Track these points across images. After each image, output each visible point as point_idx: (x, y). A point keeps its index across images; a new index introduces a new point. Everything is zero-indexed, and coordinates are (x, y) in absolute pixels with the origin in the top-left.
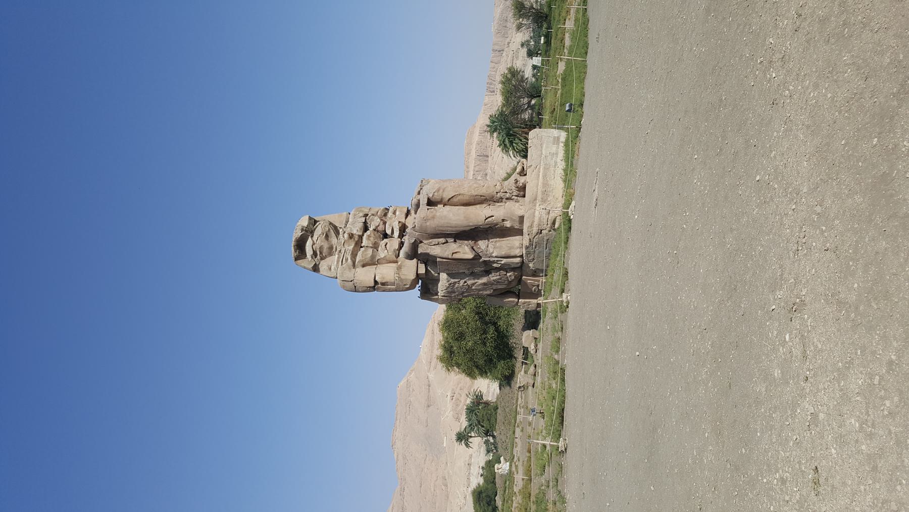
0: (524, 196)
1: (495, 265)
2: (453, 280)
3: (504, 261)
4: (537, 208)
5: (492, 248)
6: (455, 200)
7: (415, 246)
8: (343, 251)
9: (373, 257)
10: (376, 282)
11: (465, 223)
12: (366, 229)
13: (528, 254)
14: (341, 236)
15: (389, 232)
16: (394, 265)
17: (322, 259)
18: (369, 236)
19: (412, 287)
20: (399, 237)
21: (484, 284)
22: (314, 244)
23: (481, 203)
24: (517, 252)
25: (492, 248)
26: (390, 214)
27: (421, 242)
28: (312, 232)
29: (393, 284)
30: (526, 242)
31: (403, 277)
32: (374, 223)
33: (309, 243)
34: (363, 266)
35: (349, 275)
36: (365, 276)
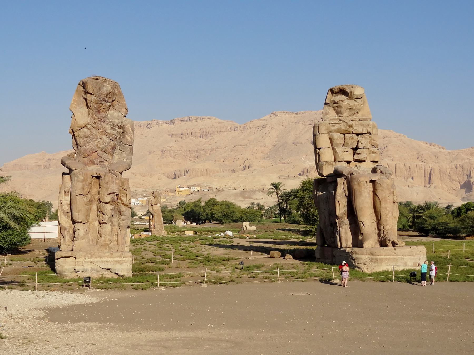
3: (338, 236)
4: (367, 256)
9: (337, 144)
10: (319, 149)
11: (358, 209)
14: (351, 118)
15: (358, 151)
16: (333, 160)
17: (333, 107)
18: (352, 138)
19: (321, 174)
23: (377, 217)
27: (345, 179)
28: (351, 98)
29: (319, 161)
30: (348, 250)
32: (364, 141)
35: (323, 130)
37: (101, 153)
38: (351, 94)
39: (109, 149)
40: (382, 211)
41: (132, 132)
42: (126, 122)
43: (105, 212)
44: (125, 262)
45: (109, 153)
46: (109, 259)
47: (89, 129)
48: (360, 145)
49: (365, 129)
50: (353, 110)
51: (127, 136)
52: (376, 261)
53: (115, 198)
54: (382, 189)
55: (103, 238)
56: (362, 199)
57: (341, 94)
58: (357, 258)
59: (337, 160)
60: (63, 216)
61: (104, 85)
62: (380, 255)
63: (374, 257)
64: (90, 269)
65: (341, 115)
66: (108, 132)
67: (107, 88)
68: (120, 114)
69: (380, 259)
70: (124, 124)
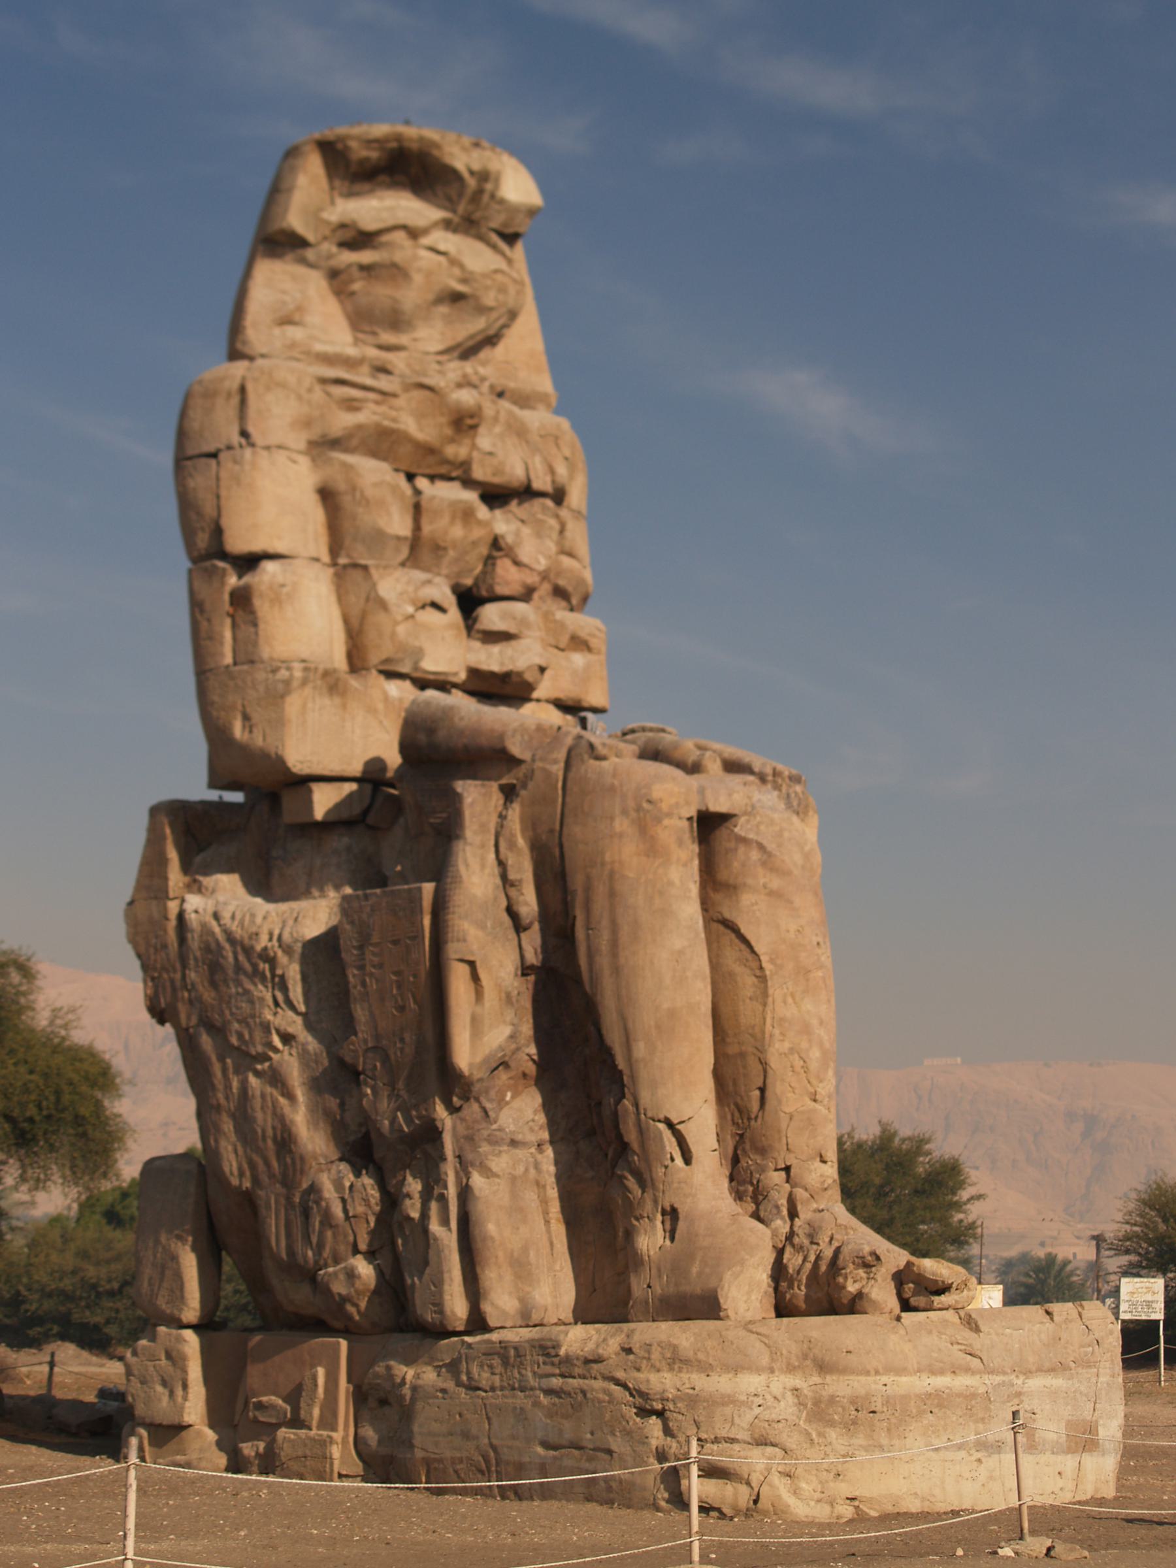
0: (783, 1309)
1: (414, 1186)
2: (293, 971)
3: (446, 1237)
4: (781, 1382)
5: (510, 1176)
6: (732, 954)
7: (490, 759)
8: (383, 383)
10: (249, 562)
11: (645, 1019)
13: (506, 1355)
14: (455, 369)
15: (491, 616)
17: (334, 274)
18: (467, 515)
20: (474, 672)
21: (285, 1141)
22: (414, 233)
24: (501, 1301)
25: (510, 1176)
27: (509, 793)
28: (468, 225)
29: (247, 655)
31: (292, 705)
34: (326, 495)
36: (275, 504)
38: (480, 192)
49: (537, 464)
50: (482, 310)
52: (860, 1416)
54: (775, 883)
56: (678, 943)
57: (395, 185)
58: (693, 1400)
59: (374, 658)
62: (890, 1369)
63: (840, 1387)
65: (387, 337)
69: (888, 1401)
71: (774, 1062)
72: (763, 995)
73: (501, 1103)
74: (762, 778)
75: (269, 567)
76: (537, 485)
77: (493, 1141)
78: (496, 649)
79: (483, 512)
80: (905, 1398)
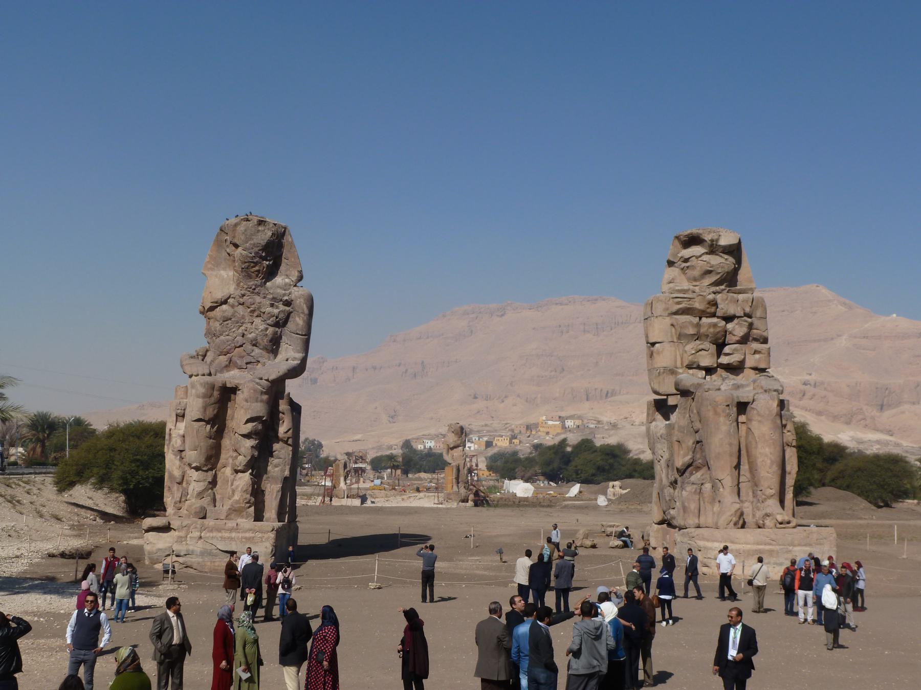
10: (653, 344)
12: (728, 319)
15: (727, 349)
17: (682, 269)
18: (715, 325)
22: (697, 257)
26: (755, 346)
33: (697, 250)
35: (659, 309)
37: (250, 347)
39: (265, 341)
40: (759, 461)
41: (306, 311)
42: (297, 293)
43: (242, 450)
44: (262, 541)
45: (265, 349)
46: (233, 535)
47: (233, 306)
48: (729, 338)
51: (297, 319)
53: (260, 427)
55: (236, 497)
58: (705, 548)
60: (173, 457)
61: (259, 231)
64: (199, 550)
65: (695, 283)
66: (263, 310)
67: (265, 235)
68: (287, 280)
70: (293, 297)
71: (759, 464)
72: (756, 448)
73: (691, 474)
74: (765, 391)
75: (657, 345)
76: (737, 315)
77: (688, 483)
78: (727, 357)
79: (724, 323)
80: (749, 551)
